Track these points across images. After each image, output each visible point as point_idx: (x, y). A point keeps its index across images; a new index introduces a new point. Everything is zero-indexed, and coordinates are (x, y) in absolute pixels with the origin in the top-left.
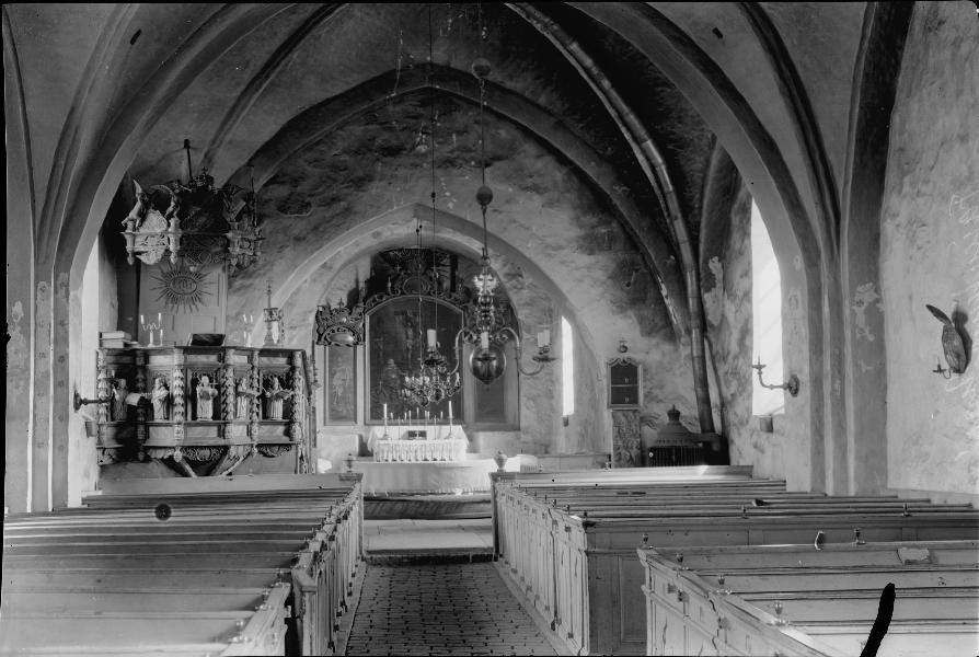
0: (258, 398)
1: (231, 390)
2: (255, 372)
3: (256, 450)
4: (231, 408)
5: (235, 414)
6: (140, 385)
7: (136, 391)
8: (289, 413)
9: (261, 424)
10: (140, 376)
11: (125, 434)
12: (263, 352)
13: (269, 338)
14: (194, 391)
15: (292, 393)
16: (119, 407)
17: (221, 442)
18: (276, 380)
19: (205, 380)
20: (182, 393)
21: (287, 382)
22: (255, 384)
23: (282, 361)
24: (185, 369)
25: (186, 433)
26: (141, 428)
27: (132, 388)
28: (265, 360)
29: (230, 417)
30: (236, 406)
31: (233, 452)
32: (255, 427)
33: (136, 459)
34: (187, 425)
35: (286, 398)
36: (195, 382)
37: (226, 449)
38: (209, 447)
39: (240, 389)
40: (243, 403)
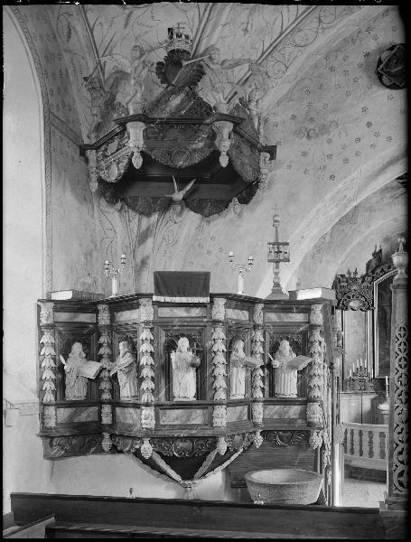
0: (262, 367)
1: (220, 358)
2: (259, 336)
3: (259, 440)
4: (221, 383)
5: (228, 391)
6: (102, 351)
7: (99, 358)
8: (304, 388)
9: (266, 403)
10: (103, 339)
11: (87, 415)
12: (269, 304)
13: (277, 285)
14: (169, 361)
15: (309, 360)
16: (70, 380)
17: (209, 433)
18: (286, 346)
19: (184, 343)
20: (151, 361)
21: (302, 347)
22: (259, 349)
23: (298, 317)
24: (156, 325)
25: (157, 418)
26: (107, 409)
27: (92, 356)
28: (273, 317)
29: (221, 395)
30: (228, 380)
31: (223, 446)
32: (259, 409)
33: (100, 451)
34: (159, 406)
35: (301, 368)
36: (171, 346)
37: (213, 442)
38: (191, 438)
39: (233, 357)
40: (240, 376)
